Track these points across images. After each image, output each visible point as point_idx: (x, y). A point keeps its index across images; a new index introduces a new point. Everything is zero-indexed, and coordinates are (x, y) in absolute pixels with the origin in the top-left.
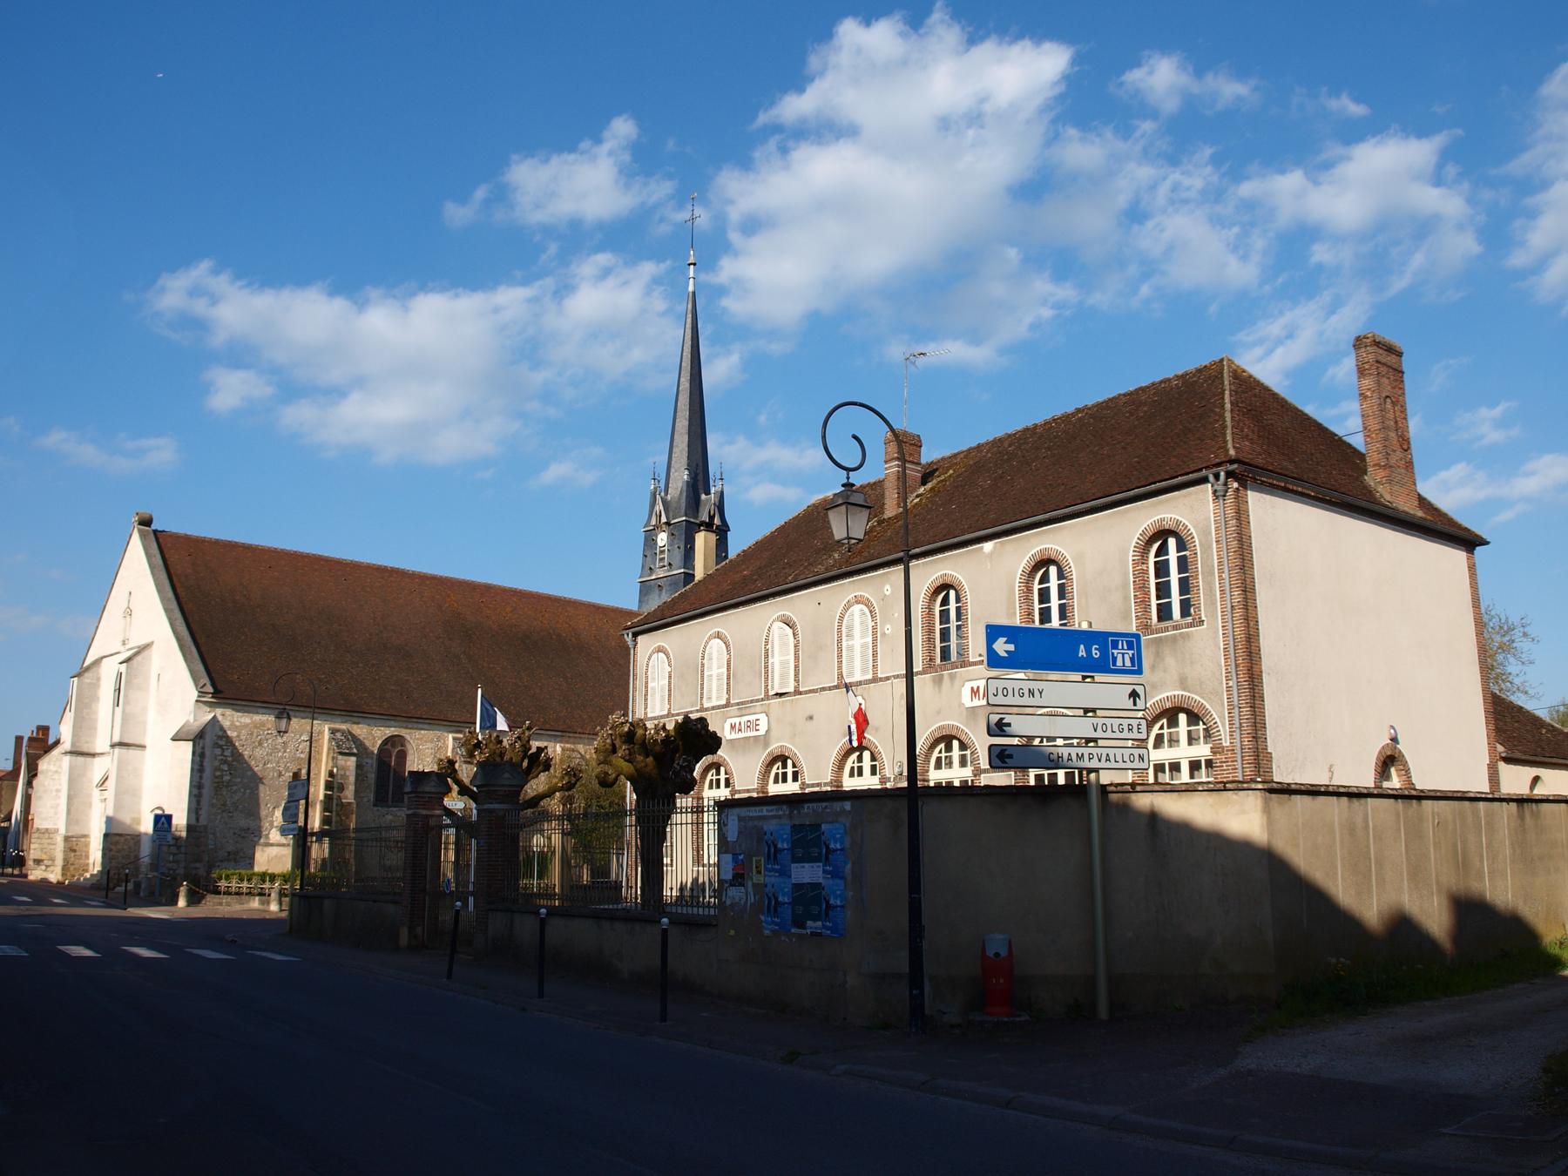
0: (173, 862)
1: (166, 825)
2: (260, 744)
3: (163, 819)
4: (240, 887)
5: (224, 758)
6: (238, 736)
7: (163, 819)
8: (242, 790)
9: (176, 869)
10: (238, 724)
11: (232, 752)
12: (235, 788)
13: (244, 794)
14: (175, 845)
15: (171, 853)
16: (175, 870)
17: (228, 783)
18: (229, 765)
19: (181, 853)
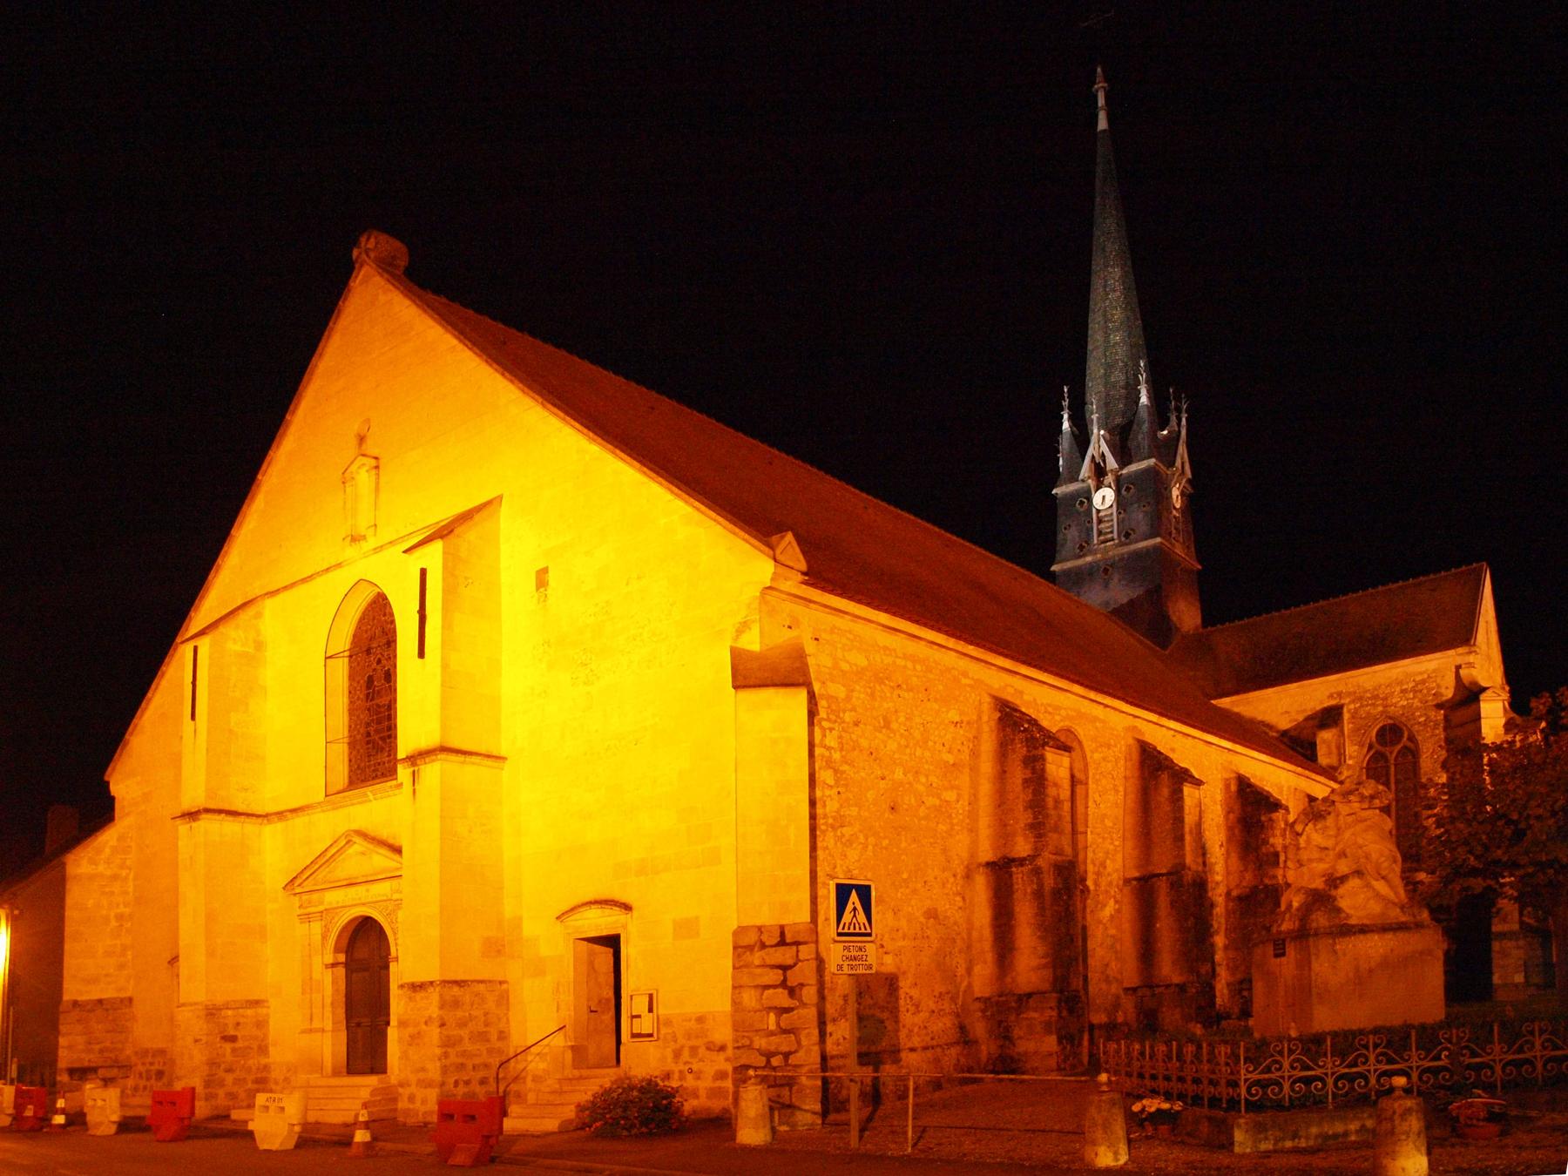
0: (786, 1032)
1: (862, 917)
2: (887, 725)
3: (854, 897)
4: (1307, 1081)
5: (827, 754)
6: (848, 698)
7: (854, 897)
8: (862, 839)
9: (790, 1053)
10: (845, 666)
11: (840, 737)
12: (847, 831)
13: (865, 847)
14: (784, 984)
15: (770, 1009)
16: (787, 1055)
17: (834, 819)
18: (836, 771)
19: (804, 1005)
